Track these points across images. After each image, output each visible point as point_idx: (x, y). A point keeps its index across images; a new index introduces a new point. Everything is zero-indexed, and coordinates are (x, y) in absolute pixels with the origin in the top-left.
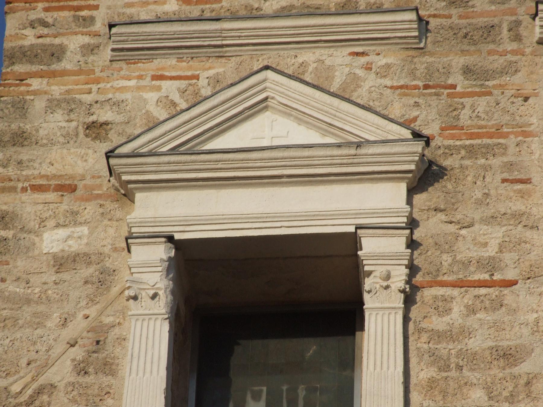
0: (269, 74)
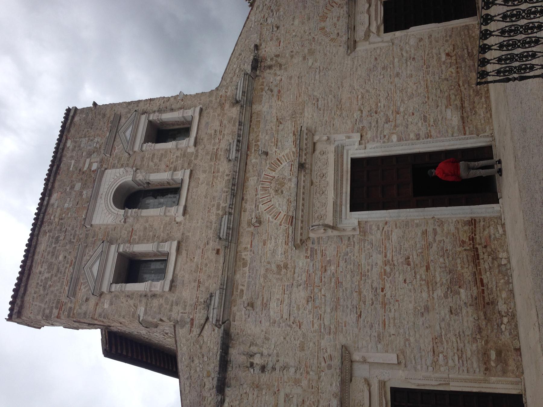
0: (85, 268)
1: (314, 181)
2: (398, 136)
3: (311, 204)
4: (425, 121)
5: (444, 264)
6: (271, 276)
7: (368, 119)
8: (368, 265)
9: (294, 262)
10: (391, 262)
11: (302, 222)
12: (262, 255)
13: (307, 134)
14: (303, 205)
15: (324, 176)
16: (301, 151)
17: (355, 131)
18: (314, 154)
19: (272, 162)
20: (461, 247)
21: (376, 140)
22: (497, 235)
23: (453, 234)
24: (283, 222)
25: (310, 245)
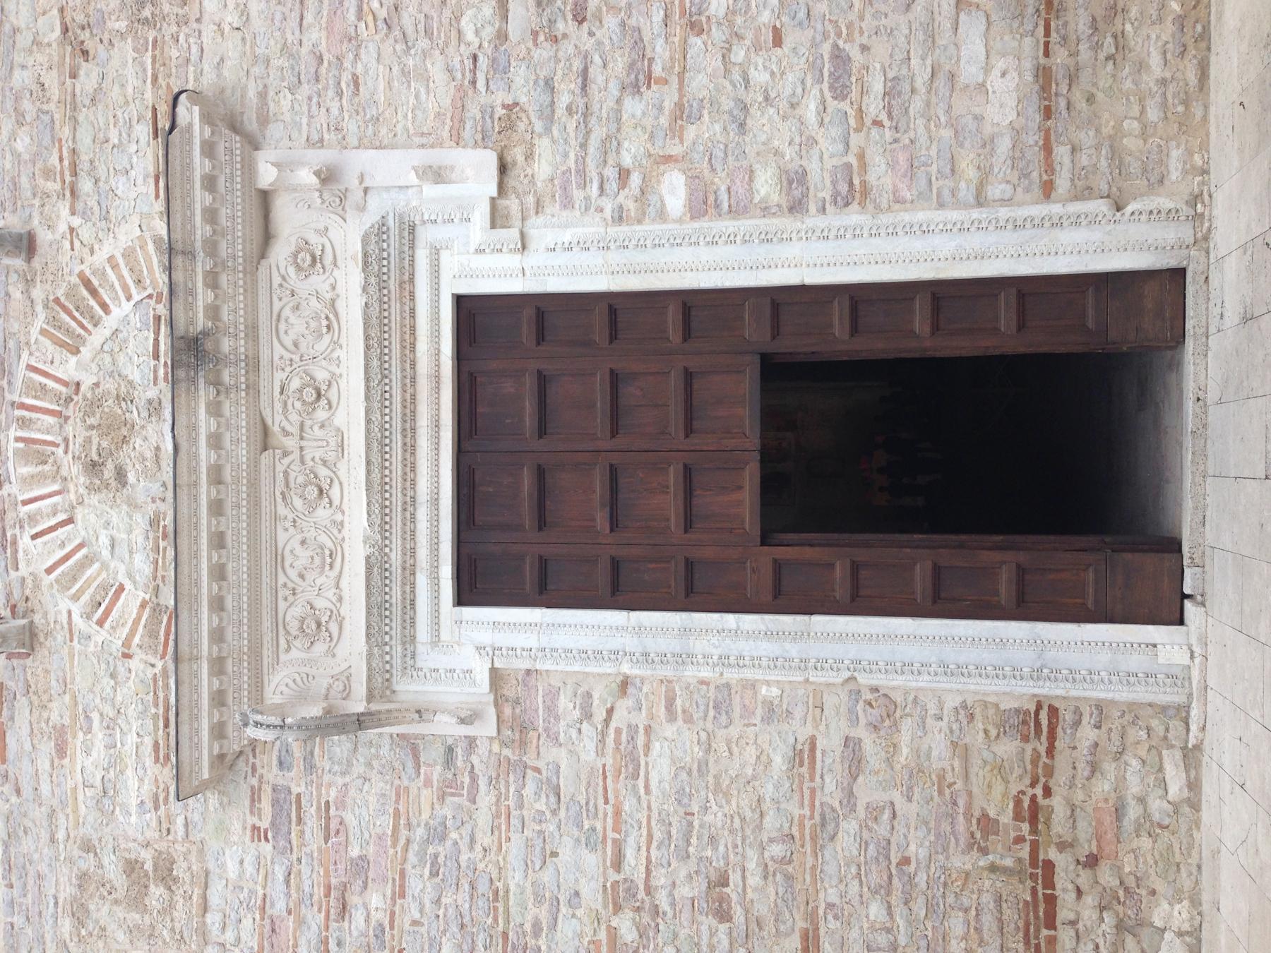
1: (276, 422)
2: (693, 179)
3: (266, 558)
4: (840, 92)
5: (888, 931)
6: (105, 909)
7: (536, 53)
8: (539, 899)
9: (201, 851)
10: (641, 894)
11: (218, 666)
12: (55, 802)
13: (209, 149)
14: (219, 573)
15: (323, 402)
16: (179, 261)
17: (467, 133)
18: (263, 262)
19: (60, 293)
20: (975, 853)
21: (578, 195)
22: (1157, 806)
23: (941, 778)
24: (137, 640)
25: (272, 774)
